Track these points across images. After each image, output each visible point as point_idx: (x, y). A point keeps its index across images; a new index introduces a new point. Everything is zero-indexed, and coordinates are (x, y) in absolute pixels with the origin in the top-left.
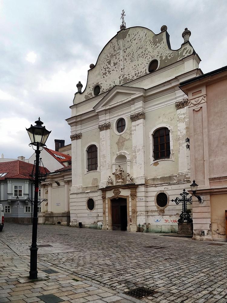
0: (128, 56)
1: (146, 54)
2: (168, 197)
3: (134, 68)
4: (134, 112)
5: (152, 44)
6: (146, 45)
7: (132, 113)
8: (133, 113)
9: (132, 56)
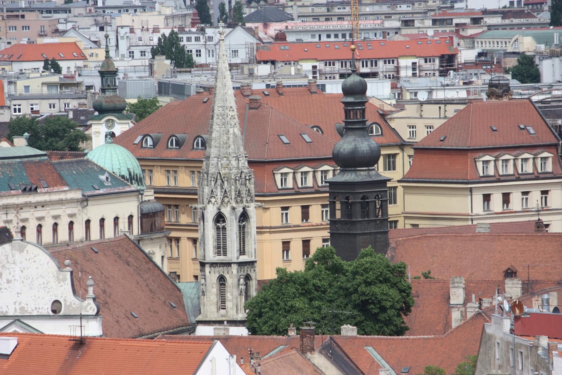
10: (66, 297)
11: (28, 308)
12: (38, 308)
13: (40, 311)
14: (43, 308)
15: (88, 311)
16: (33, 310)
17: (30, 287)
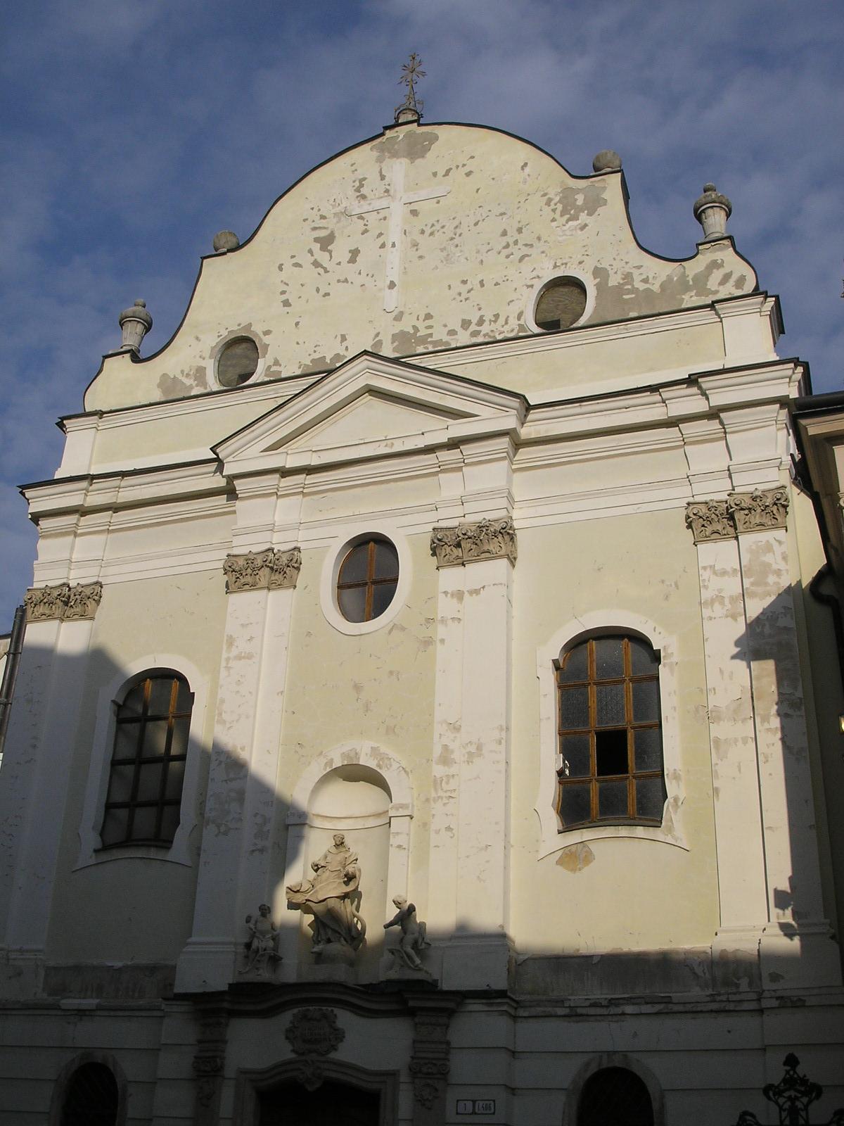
0: (432, 234)
1: (526, 245)
2: (655, 1106)
3: (460, 294)
4: (459, 511)
7: (442, 513)
9: (452, 239)
11: (431, 327)
12: (475, 321)
13: (485, 328)
14: (497, 316)
15: (717, 292)
16: (452, 333)
17: (445, 254)
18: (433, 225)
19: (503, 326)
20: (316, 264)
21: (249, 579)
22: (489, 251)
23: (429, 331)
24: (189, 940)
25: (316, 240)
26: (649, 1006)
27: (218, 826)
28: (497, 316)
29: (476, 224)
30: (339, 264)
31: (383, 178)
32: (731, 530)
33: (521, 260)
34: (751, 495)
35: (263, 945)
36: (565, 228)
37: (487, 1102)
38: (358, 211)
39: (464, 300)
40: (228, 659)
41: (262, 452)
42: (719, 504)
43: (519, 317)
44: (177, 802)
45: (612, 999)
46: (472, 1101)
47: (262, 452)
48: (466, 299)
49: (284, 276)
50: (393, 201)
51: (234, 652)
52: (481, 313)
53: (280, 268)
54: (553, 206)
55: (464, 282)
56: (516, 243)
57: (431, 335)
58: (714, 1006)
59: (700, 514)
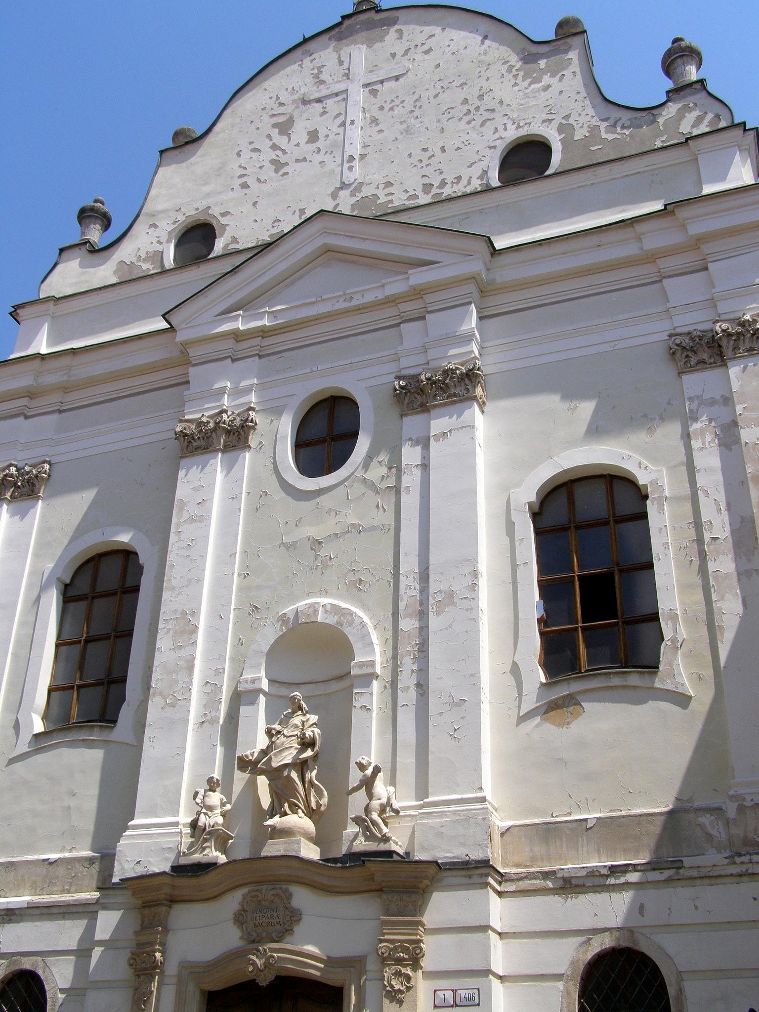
0: (392, 109)
5: (516, 76)
6: (485, 75)
8: (411, 364)
10: (567, 117)
14: (459, 178)
16: (416, 197)
17: (404, 126)
18: (393, 101)
19: (465, 187)
20: (275, 147)
21: (202, 443)
22: (450, 119)
23: (390, 198)
24: (131, 823)
25: (274, 126)
26: (657, 872)
27: (165, 698)
28: (459, 178)
29: (436, 96)
30: (298, 145)
31: (341, 63)
32: (718, 358)
33: (482, 125)
34: (738, 321)
35: (212, 821)
36: (527, 91)
37: (470, 991)
38: (317, 95)
39: (425, 167)
40: (179, 525)
41: (216, 316)
42: (703, 333)
43: (481, 178)
44: (123, 680)
45: (612, 866)
46: (453, 991)
47: (216, 316)
48: (427, 165)
49: (242, 161)
50: (351, 83)
51: (185, 516)
52: (443, 177)
53: (239, 154)
54: (514, 72)
55: (425, 150)
56: (477, 109)
57: (392, 201)
58: (734, 870)
59: (684, 344)
